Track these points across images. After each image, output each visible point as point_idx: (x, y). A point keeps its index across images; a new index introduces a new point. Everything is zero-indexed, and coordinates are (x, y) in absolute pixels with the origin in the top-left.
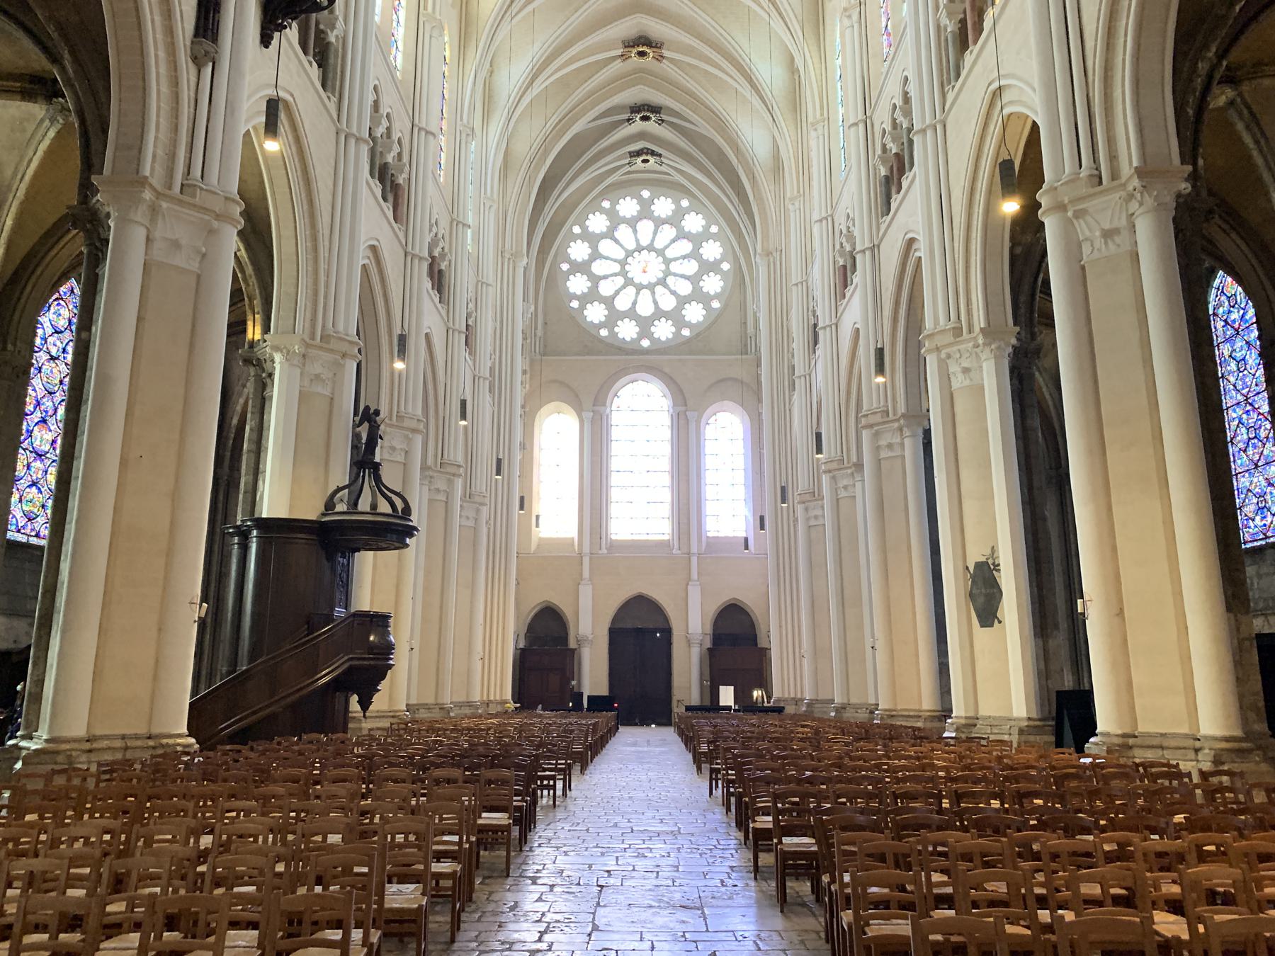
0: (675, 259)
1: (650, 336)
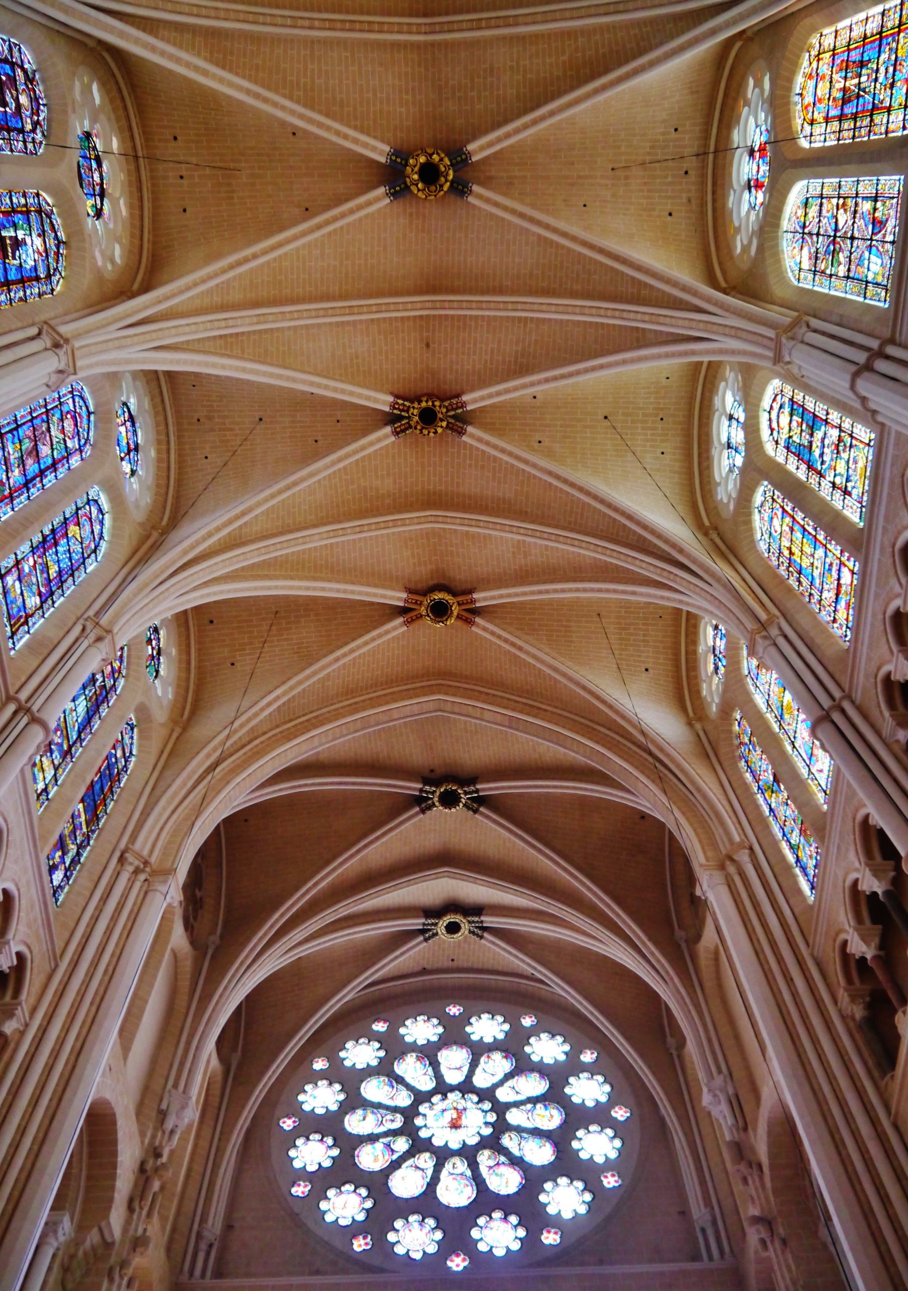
0: (517, 1104)
1: (468, 1247)
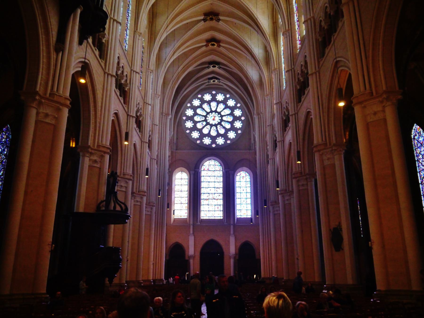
0: (225, 116)
1: (215, 143)
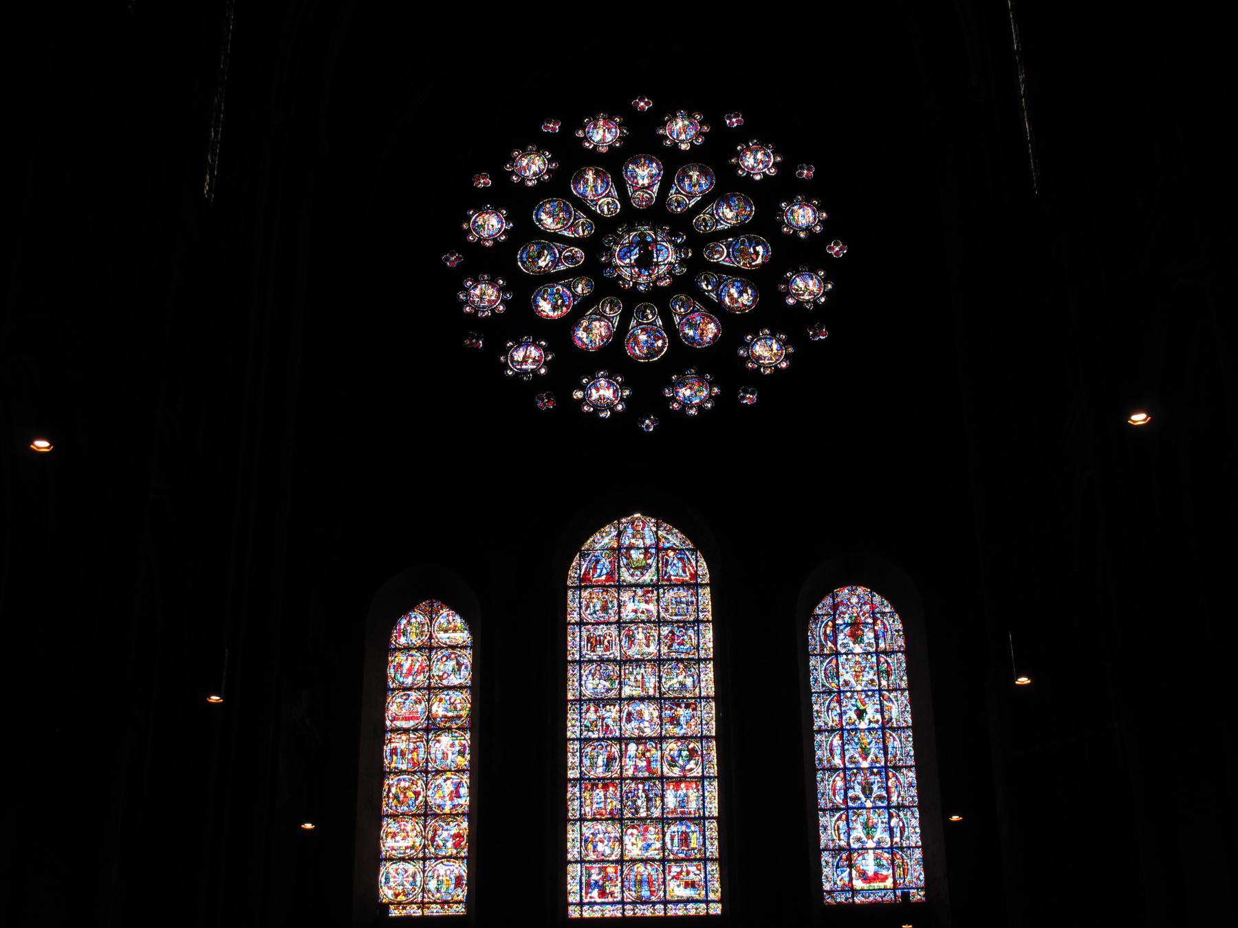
1: (660, 406)
